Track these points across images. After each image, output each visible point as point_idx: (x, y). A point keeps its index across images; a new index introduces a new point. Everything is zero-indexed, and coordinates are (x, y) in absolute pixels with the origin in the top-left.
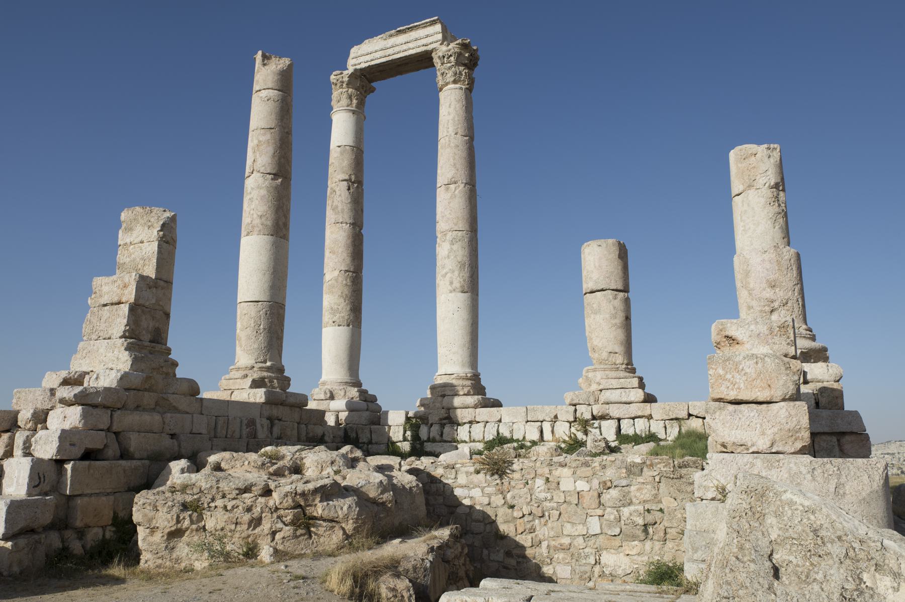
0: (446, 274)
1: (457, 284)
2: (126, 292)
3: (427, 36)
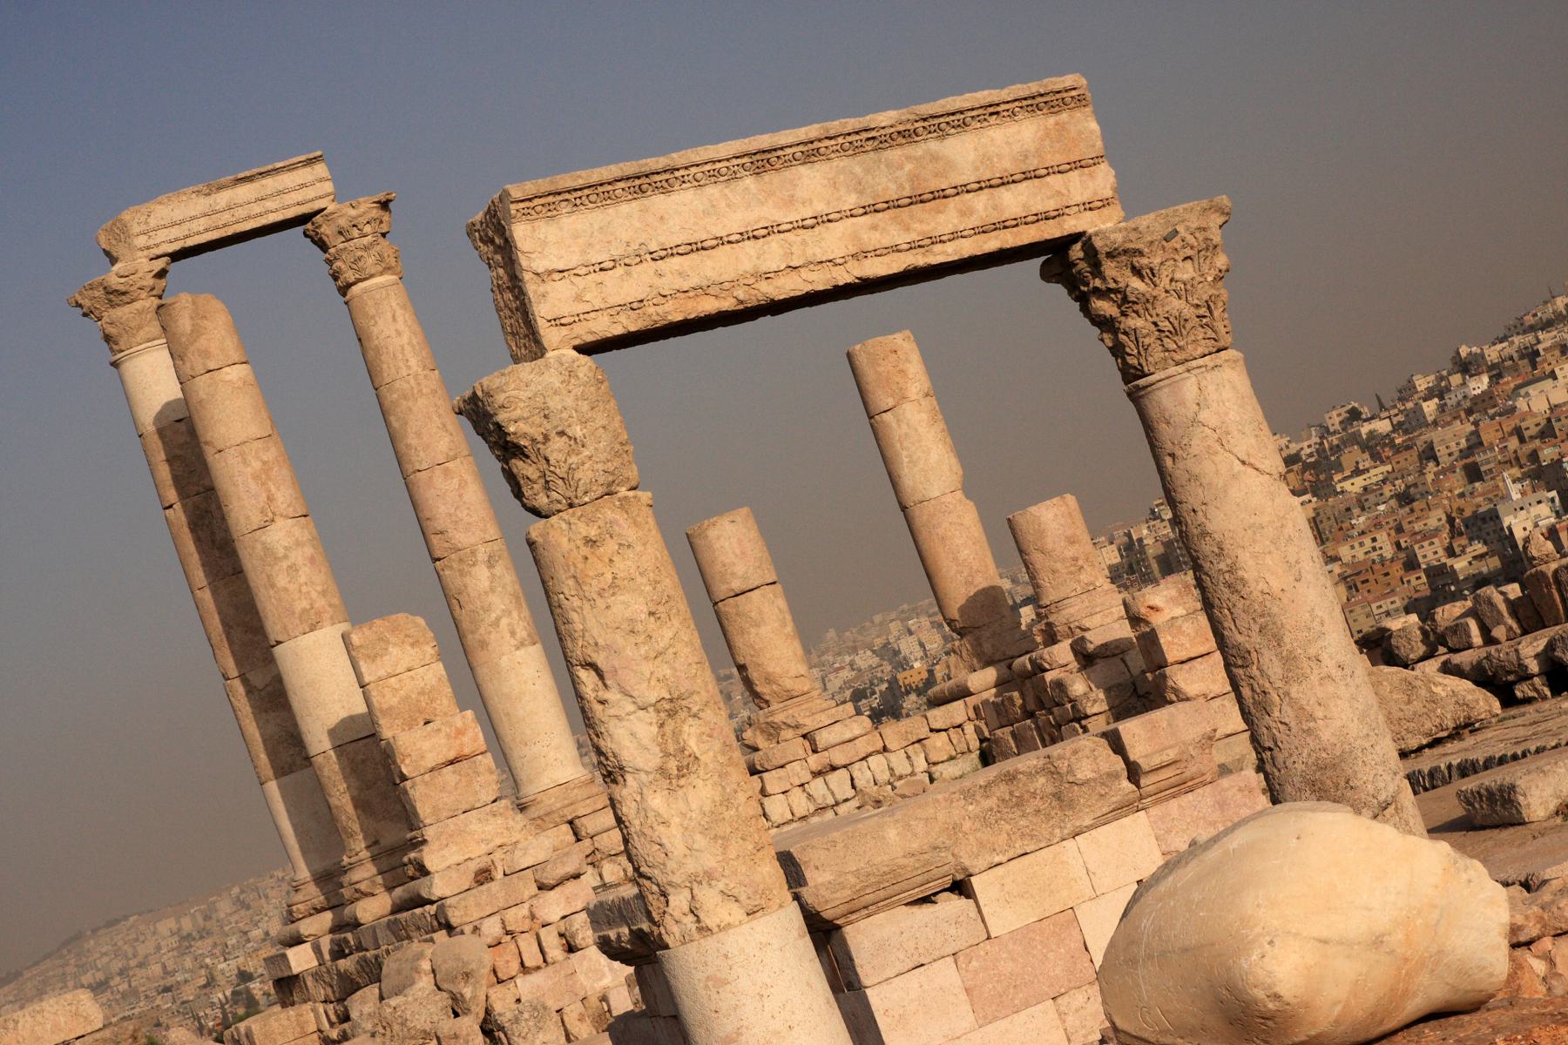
0: (498, 619)
1: (522, 633)
2: (465, 739)
3: (303, 186)
